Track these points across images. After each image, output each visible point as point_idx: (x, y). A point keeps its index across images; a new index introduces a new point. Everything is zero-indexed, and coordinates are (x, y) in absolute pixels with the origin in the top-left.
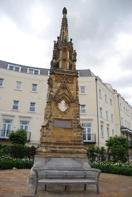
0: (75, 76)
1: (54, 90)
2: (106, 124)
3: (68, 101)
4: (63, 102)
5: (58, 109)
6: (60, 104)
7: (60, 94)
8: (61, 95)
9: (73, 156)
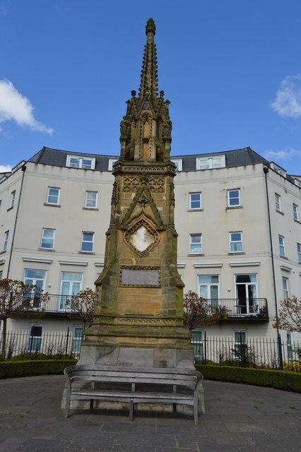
0: (166, 174)
1: (122, 208)
3: (152, 230)
6: (134, 236)
8: (135, 217)
9: (161, 341)
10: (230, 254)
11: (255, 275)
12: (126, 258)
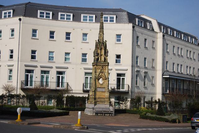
6: (100, 80)
7: (100, 75)
8: (100, 76)
12: (98, 85)
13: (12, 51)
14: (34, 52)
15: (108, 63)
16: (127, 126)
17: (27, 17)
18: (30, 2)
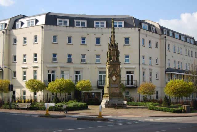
2: (148, 70)
4: (114, 76)
5: (113, 80)
10: (125, 63)
11: (133, 72)
13: (36, 55)
14: (54, 55)
15: (120, 62)
16: (139, 117)
17: (129, 28)
18: (49, 13)
